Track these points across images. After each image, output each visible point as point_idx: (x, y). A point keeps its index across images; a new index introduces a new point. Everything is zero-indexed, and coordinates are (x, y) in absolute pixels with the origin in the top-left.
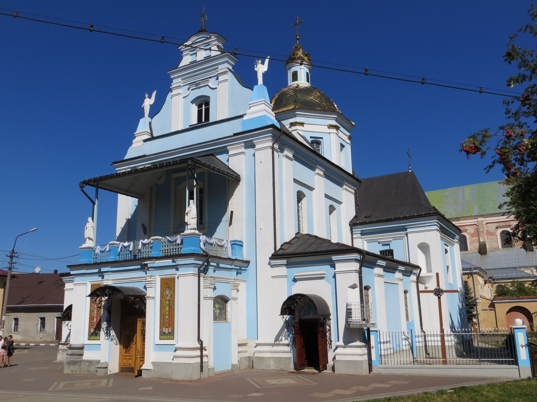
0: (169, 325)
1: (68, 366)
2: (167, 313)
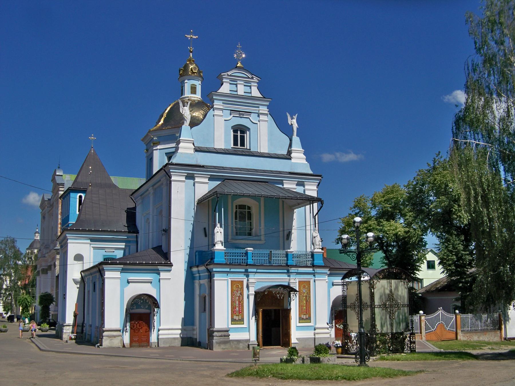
0: (306, 312)
1: (218, 345)
2: (305, 305)
